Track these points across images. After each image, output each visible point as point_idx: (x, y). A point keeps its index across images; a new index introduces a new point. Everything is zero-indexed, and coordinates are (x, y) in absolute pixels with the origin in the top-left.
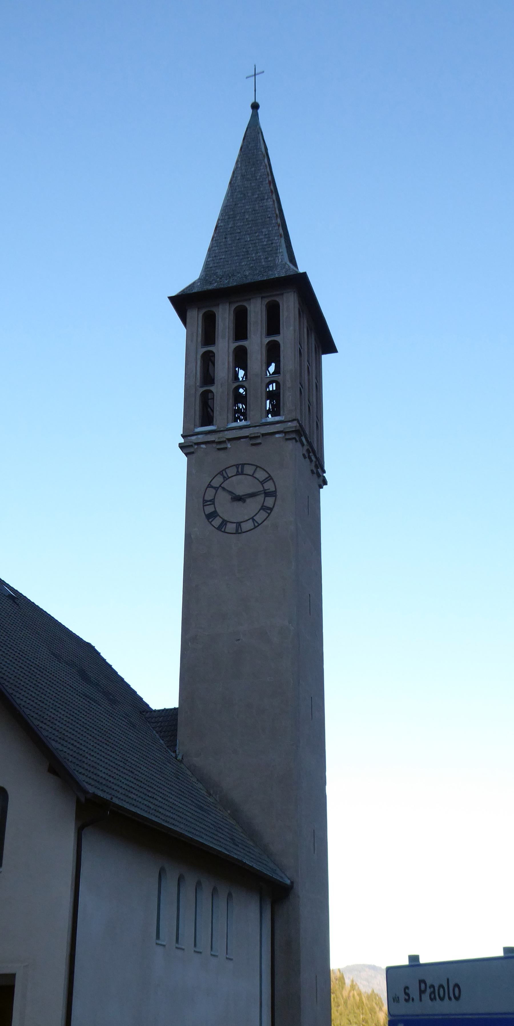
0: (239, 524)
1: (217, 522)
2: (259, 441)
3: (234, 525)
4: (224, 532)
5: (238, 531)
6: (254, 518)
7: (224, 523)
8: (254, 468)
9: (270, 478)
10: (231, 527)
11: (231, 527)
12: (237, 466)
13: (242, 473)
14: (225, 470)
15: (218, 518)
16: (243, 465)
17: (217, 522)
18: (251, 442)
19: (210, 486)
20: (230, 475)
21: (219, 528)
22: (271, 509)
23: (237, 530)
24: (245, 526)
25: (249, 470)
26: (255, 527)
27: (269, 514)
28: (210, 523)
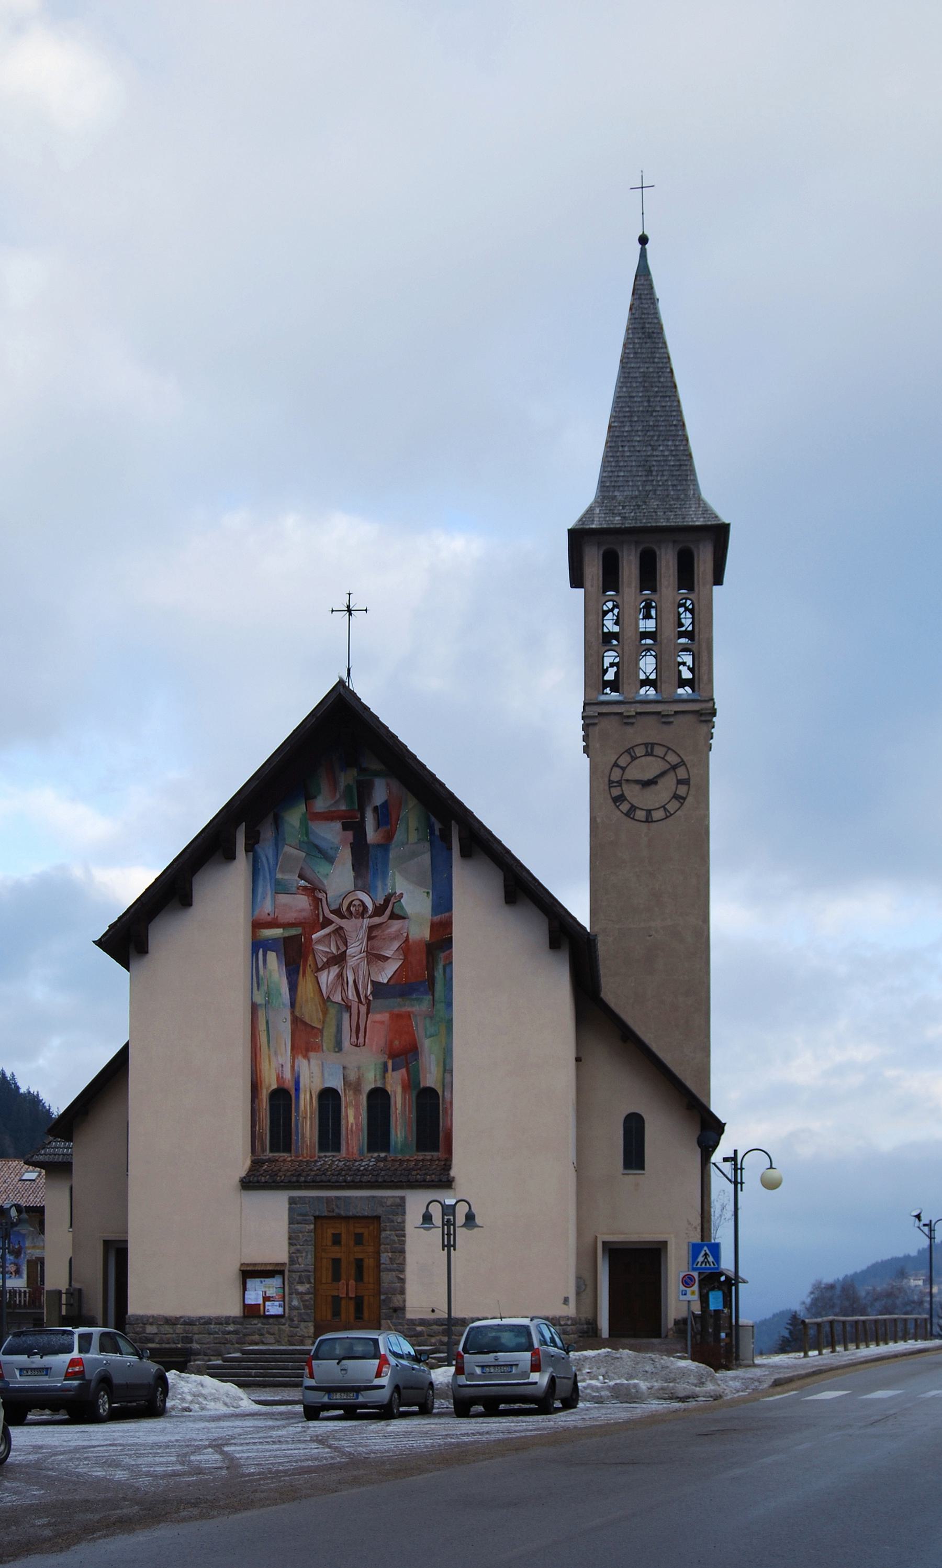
0: (649, 812)
1: (625, 807)
2: (671, 719)
3: (644, 813)
4: (633, 819)
5: (648, 820)
6: (666, 806)
7: (633, 808)
8: (665, 749)
9: (683, 763)
10: (640, 815)
11: (640, 815)
12: (646, 745)
13: (651, 754)
14: (632, 748)
15: (626, 802)
16: (653, 744)
17: (625, 807)
18: (663, 720)
19: (616, 765)
20: (638, 755)
21: (627, 814)
22: (684, 799)
23: (647, 818)
24: (657, 815)
25: (659, 751)
26: (667, 817)
27: (682, 804)
28: (618, 807)
